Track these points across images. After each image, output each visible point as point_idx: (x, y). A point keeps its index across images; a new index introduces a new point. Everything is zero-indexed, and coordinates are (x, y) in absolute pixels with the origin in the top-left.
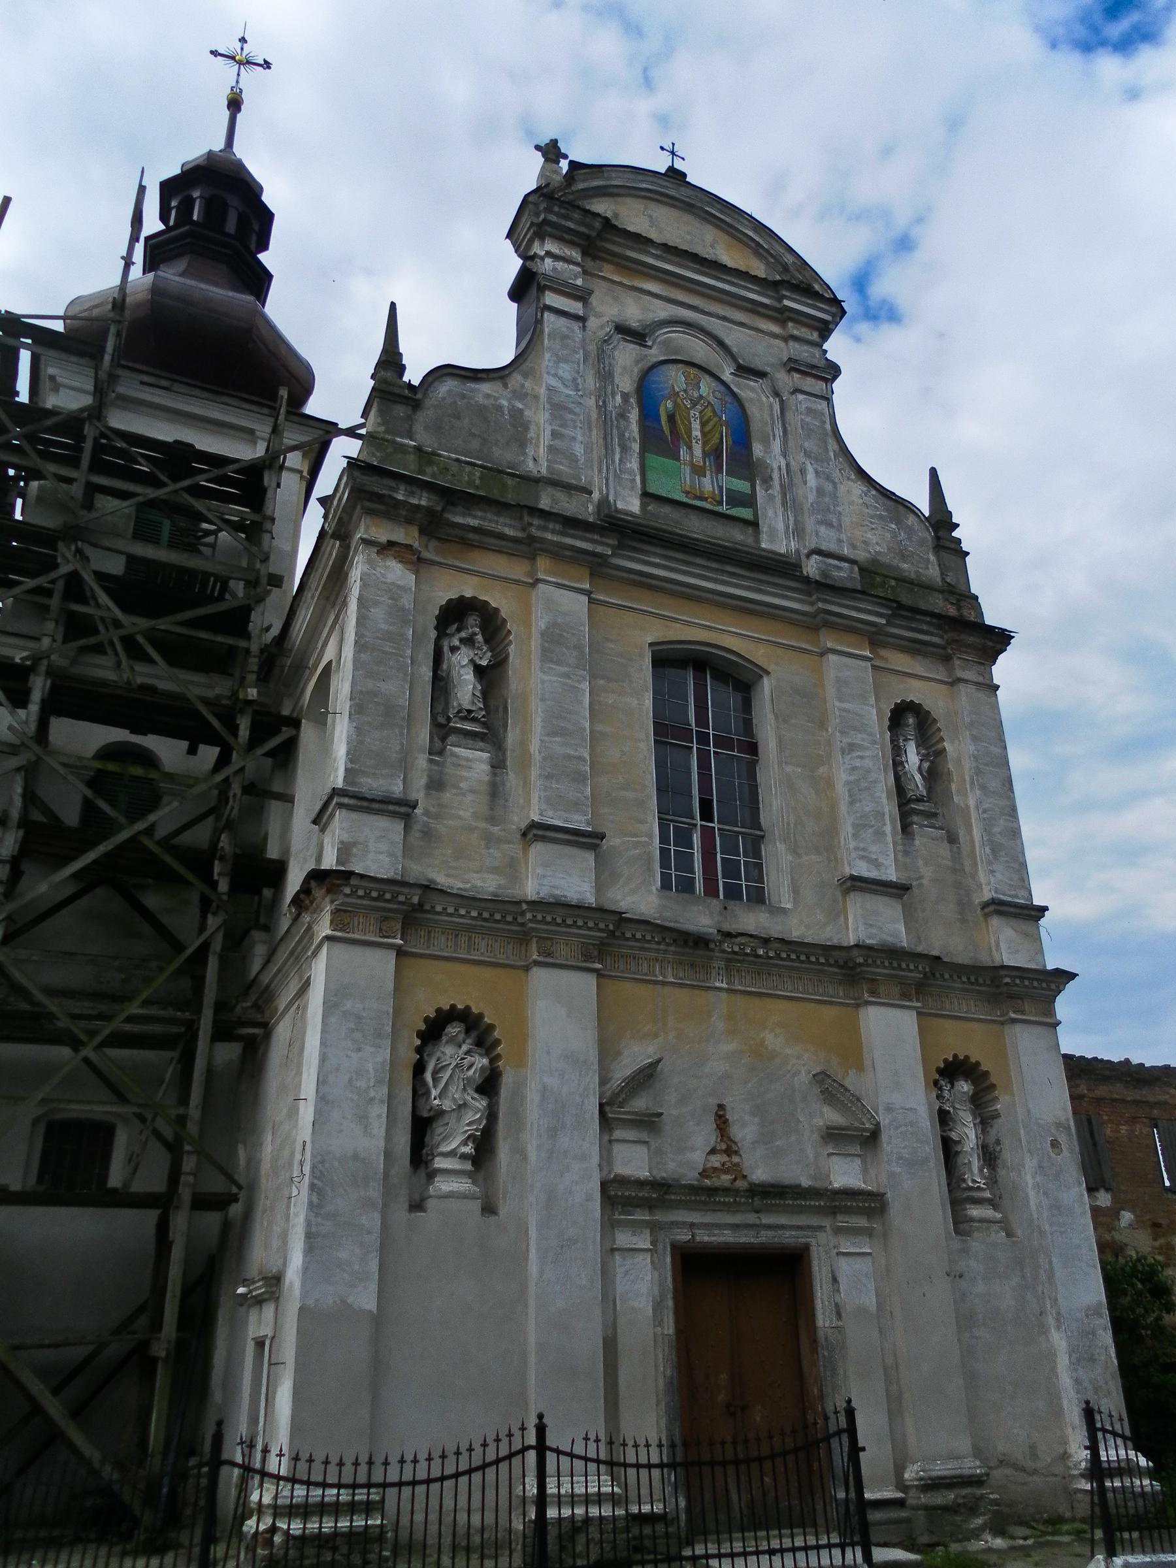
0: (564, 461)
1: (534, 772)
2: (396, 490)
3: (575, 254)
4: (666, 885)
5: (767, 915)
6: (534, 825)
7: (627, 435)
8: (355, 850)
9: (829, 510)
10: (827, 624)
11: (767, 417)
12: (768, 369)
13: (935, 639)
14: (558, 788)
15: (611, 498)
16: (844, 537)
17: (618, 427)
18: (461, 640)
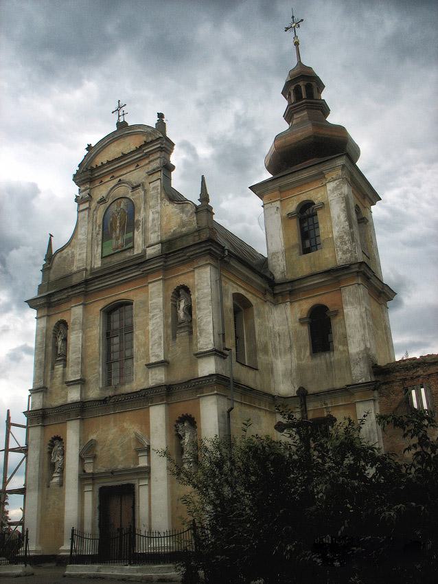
3: (88, 186)
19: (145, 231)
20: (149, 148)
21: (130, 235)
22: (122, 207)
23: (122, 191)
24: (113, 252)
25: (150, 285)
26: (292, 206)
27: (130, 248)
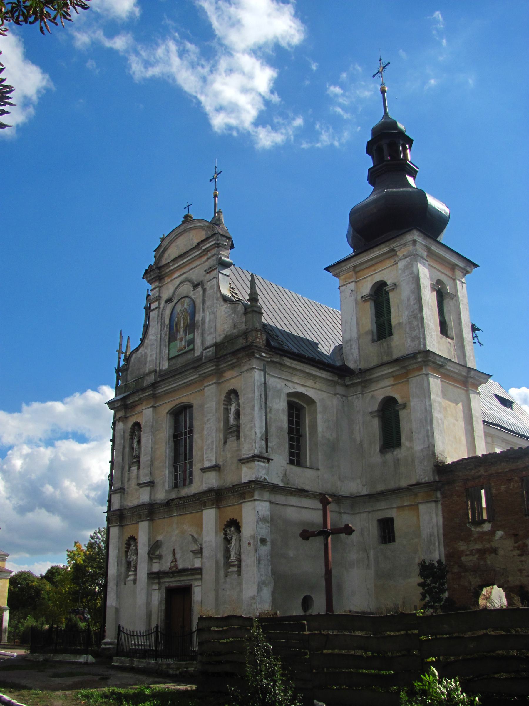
2: (115, 405)
3: (157, 284)
10: (205, 377)
12: (203, 279)
13: (235, 361)
19: (203, 334)
20: (205, 245)
21: (191, 336)
23: (186, 289)
24: (177, 354)
25: (206, 389)
26: (366, 288)
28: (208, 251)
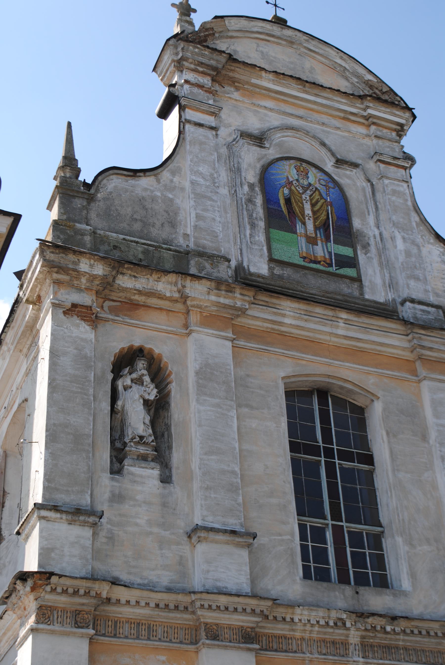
0: (208, 237)
1: (196, 485)
2: (77, 263)
4: (307, 575)
5: (392, 597)
6: (197, 529)
7: (254, 215)
8: (53, 555)
9: (415, 267)
11: (361, 197)
12: (359, 162)
14: (215, 498)
15: (245, 264)
16: (429, 288)
17: (247, 210)
18: (132, 381)
22: (312, 180)
24: (301, 262)
27: (352, 279)
28: (374, 123)
